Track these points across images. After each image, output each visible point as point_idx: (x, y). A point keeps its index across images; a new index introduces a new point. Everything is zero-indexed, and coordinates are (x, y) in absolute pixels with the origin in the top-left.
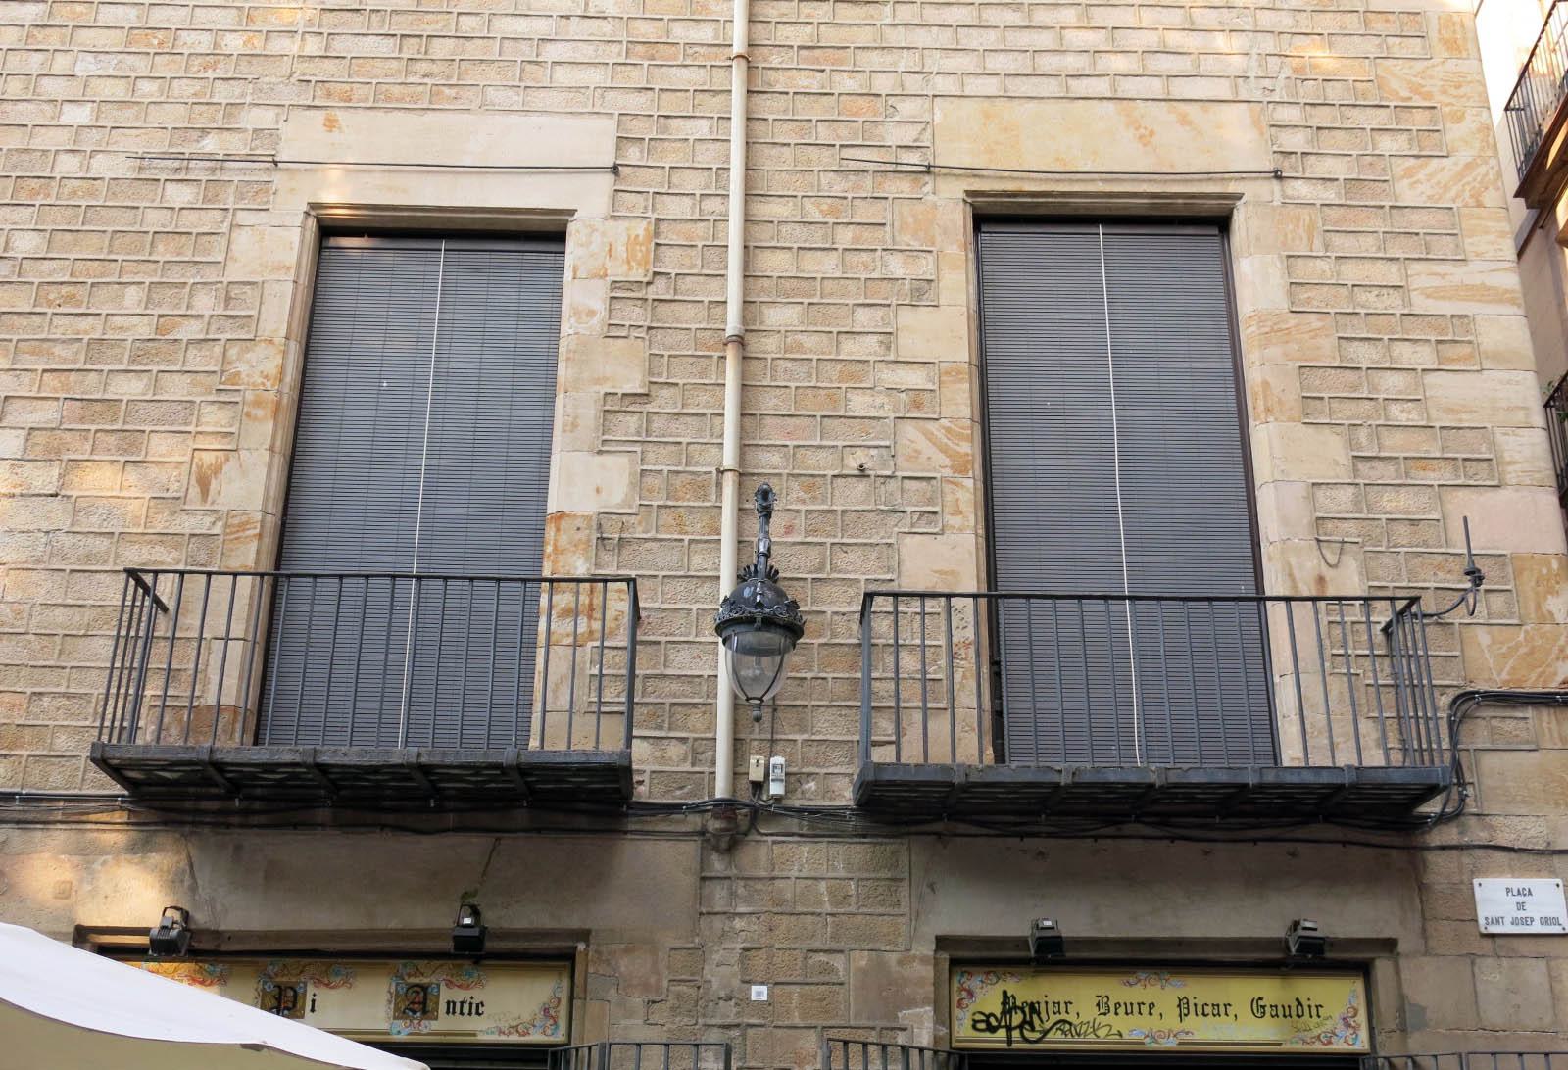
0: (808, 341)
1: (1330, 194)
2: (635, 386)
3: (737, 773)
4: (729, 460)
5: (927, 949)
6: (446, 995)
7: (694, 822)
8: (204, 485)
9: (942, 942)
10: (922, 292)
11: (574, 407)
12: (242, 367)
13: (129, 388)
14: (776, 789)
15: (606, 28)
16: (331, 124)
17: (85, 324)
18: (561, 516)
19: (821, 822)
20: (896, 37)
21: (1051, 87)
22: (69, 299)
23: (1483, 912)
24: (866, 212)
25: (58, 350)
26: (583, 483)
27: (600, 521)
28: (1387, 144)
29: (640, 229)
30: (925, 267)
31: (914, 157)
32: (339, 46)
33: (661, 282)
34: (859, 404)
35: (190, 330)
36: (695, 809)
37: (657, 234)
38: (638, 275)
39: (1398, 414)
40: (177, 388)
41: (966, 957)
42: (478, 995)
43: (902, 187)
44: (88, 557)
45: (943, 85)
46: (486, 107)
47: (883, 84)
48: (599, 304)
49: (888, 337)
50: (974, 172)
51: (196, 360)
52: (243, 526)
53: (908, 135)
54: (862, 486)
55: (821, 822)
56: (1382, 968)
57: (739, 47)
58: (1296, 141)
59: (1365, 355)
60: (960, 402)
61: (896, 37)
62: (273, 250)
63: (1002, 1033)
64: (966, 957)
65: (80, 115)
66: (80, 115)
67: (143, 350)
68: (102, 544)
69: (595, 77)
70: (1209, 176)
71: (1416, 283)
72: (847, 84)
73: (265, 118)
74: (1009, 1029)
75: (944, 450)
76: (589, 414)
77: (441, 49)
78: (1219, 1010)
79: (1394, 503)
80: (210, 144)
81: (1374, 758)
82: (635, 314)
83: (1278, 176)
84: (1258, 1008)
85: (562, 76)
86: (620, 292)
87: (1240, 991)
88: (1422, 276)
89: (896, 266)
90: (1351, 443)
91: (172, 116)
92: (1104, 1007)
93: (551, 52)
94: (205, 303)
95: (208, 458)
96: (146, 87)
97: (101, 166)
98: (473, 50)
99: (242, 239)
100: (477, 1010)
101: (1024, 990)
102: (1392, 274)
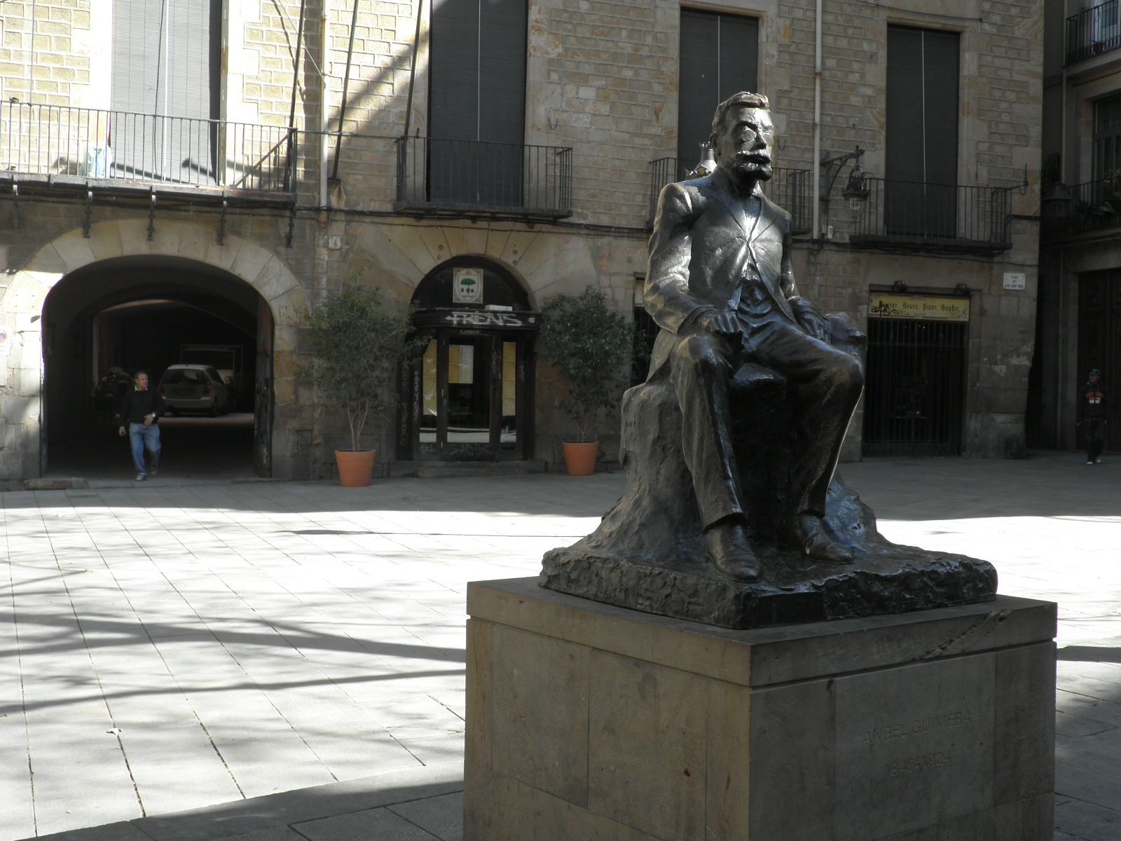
2: (786, 87)
3: (820, 230)
4: (817, 119)
7: (805, 246)
8: (657, 114)
9: (871, 285)
10: (872, 57)
12: (664, 69)
13: (628, 74)
14: (830, 236)
17: (610, 44)
19: (840, 246)
23: (1005, 283)
24: (857, 22)
28: (1014, 11)
29: (788, 23)
30: (874, 47)
33: (794, 46)
34: (854, 100)
35: (645, 52)
36: (807, 241)
37: (792, 24)
38: (787, 41)
39: (1005, 117)
40: (644, 75)
41: (875, 290)
43: (867, 13)
48: (776, 54)
49: (862, 76)
50: (891, 9)
52: (671, 132)
54: (853, 132)
55: (840, 246)
56: (976, 298)
59: (997, 94)
60: (882, 104)
63: (879, 312)
64: (875, 290)
68: (627, 136)
74: (881, 311)
75: (877, 120)
78: (933, 308)
79: (999, 149)
83: (981, 20)
84: (943, 308)
86: (782, 49)
87: (939, 302)
89: (865, 46)
92: (904, 305)
94: (649, 40)
95: (657, 105)
99: (659, 13)
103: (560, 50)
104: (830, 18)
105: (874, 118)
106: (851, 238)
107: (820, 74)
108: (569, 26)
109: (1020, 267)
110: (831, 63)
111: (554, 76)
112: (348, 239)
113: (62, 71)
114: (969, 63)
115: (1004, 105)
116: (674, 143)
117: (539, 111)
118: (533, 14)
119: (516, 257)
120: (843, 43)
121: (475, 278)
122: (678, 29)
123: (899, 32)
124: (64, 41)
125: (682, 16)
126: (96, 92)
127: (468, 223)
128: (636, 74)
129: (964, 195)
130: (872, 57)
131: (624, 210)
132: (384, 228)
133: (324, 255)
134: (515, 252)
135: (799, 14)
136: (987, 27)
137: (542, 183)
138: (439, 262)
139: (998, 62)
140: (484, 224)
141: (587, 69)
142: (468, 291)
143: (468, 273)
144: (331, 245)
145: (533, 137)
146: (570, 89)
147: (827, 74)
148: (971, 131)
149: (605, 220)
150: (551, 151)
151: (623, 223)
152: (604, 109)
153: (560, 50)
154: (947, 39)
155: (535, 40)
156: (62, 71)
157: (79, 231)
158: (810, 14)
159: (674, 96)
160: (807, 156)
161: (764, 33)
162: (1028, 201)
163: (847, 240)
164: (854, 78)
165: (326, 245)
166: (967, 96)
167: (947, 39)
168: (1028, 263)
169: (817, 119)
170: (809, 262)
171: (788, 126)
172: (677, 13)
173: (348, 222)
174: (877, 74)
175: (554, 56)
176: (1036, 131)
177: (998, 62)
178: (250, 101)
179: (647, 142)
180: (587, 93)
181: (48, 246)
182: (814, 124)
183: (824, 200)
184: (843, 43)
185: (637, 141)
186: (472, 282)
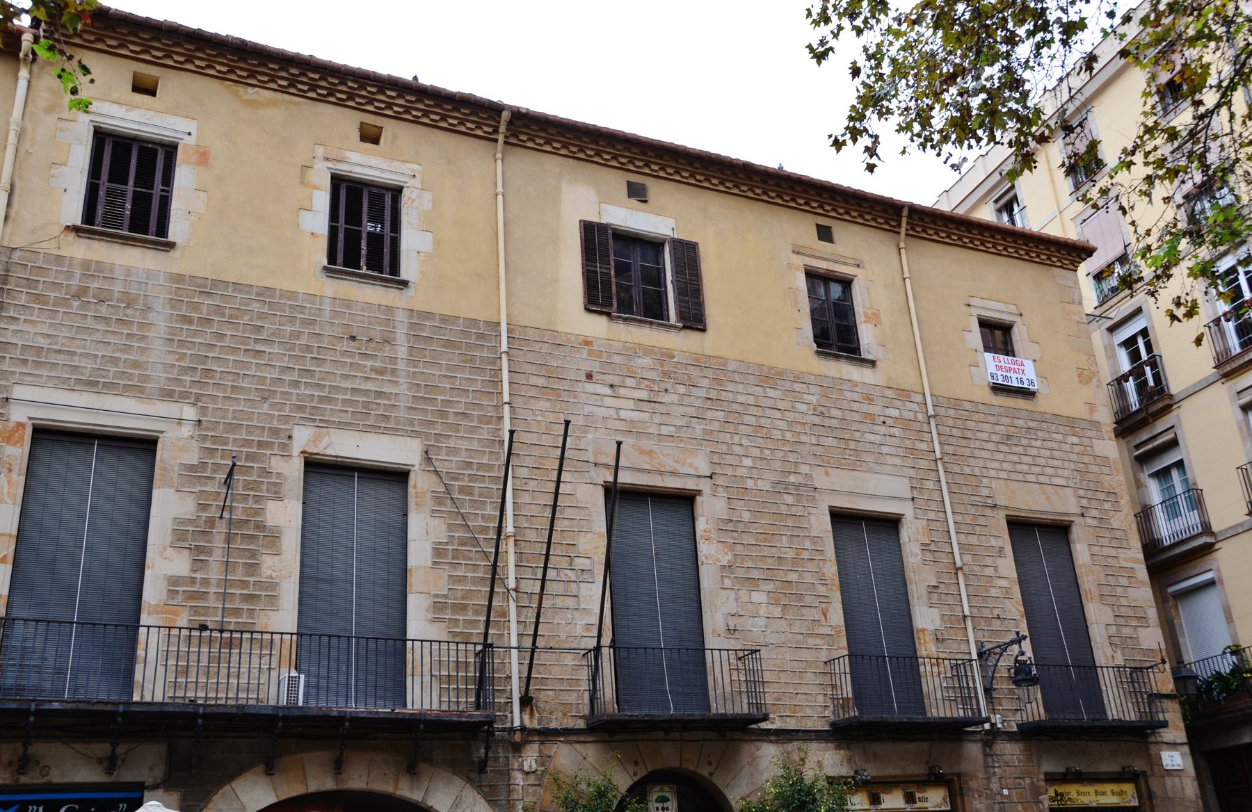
0: (976, 568)
1: (1095, 523)
5: (1042, 777)
6: (918, 795)
7: (979, 737)
8: (825, 615)
9: (1046, 774)
11: (917, 591)
12: (824, 570)
13: (793, 577)
15: (897, 441)
16: (827, 473)
17: (774, 550)
18: (923, 630)
20: (977, 453)
21: (1020, 477)
22: (765, 540)
23: (1164, 763)
24: (982, 521)
25: (768, 560)
26: (925, 618)
27: (935, 632)
28: (1107, 506)
31: (989, 501)
32: (823, 441)
34: (993, 592)
39: (1124, 602)
42: (926, 795)
43: (988, 512)
44: (797, 642)
45: (993, 473)
46: (870, 471)
47: (977, 471)
50: (1007, 508)
51: (811, 567)
53: (985, 492)
54: (999, 622)
55: (1011, 737)
57: (938, 455)
58: (1084, 502)
59: (1112, 580)
61: (977, 453)
62: (823, 524)
65: (748, 462)
66: (748, 462)
67: (796, 560)
68: (800, 637)
69: (898, 461)
70: (1066, 514)
71: (1121, 556)
72: (967, 471)
73: (804, 469)
76: (924, 592)
77: (852, 445)
78: (1104, 793)
79: (1126, 631)
80: (792, 478)
81: (1133, 718)
82: (929, 556)
83: (1082, 515)
84: (1113, 793)
85: (890, 460)
87: (1108, 787)
88: (1122, 554)
89: (993, 542)
90: (1113, 611)
91: (777, 465)
93: (885, 449)
94: (807, 544)
96: (767, 452)
97: (761, 485)
98: (861, 447)
99: (812, 518)
100: (926, 800)
101: (1060, 789)
102: (1112, 552)
103: (729, 557)
104: (959, 518)
105: (1014, 608)
106: (1018, 725)
107: (961, 568)
108: (735, 534)
109: (1173, 745)
110: (967, 558)
111: (728, 583)
112: (543, 759)
113: (250, 598)
114: (1081, 552)
115: (1120, 590)
116: (844, 642)
117: (714, 620)
118: (701, 525)
119: (710, 769)
120: (973, 540)
121: (668, 795)
122: (831, 535)
123: (1020, 527)
124: (253, 568)
125: (832, 522)
126: (284, 617)
127: (661, 735)
128: (801, 576)
129: (1107, 680)
130: (1001, 550)
131: (809, 712)
132: (578, 746)
133: (518, 778)
134: (710, 763)
135: (932, 515)
136: (1089, 520)
137: (728, 689)
138: (636, 779)
139: (1106, 551)
140: (676, 735)
141: (755, 574)
142: (663, 809)
143: (662, 790)
144: (526, 768)
145: (711, 641)
146: (744, 595)
147: (966, 568)
148: (1098, 616)
149: (791, 725)
150: (732, 656)
151: (809, 725)
152: (777, 611)
153: (729, 557)
154: (1059, 531)
155: (704, 548)
156: (250, 598)
157: (260, 768)
158: (941, 515)
159: (837, 596)
160: (964, 648)
161: (906, 533)
162: (1164, 681)
163: (1015, 729)
164: (989, 571)
165: (521, 770)
166: (1088, 582)
167: (1059, 531)
168: (1179, 741)
169: (967, 612)
170: (986, 755)
171: (942, 619)
172: (828, 519)
173: (542, 743)
174: (1007, 566)
175: (725, 563)
176: (1152, 613)
177: (1106, 551)
178: (436, 620)
179: (819, 641)
180: (759, 597)
181: (227, 787)
182: (965, 617)
183: (988, 691)
184: (973, 540)
185: (812, 642)
186: (667, 800)
